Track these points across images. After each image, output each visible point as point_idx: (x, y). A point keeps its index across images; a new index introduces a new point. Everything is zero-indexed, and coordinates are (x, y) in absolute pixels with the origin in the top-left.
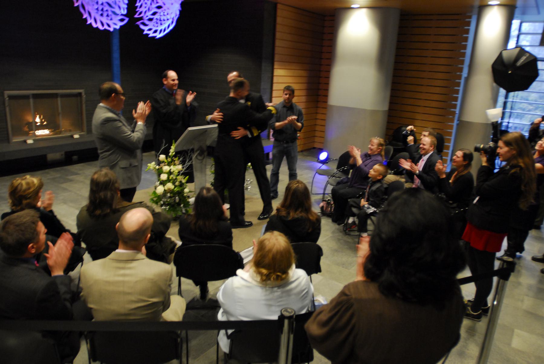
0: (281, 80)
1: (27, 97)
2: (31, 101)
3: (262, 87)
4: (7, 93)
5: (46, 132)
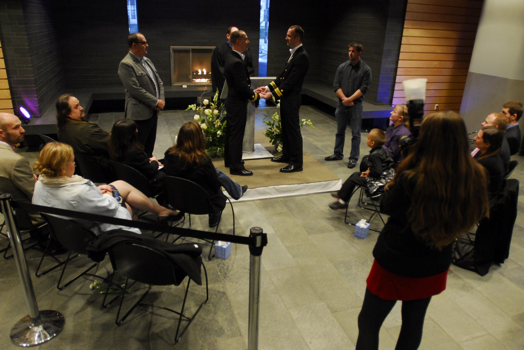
0: (412, 41)
1: (187, 51)
2: (191, 54)
3: (385, 48)
4: (172, 47)
5: (204, 81)
